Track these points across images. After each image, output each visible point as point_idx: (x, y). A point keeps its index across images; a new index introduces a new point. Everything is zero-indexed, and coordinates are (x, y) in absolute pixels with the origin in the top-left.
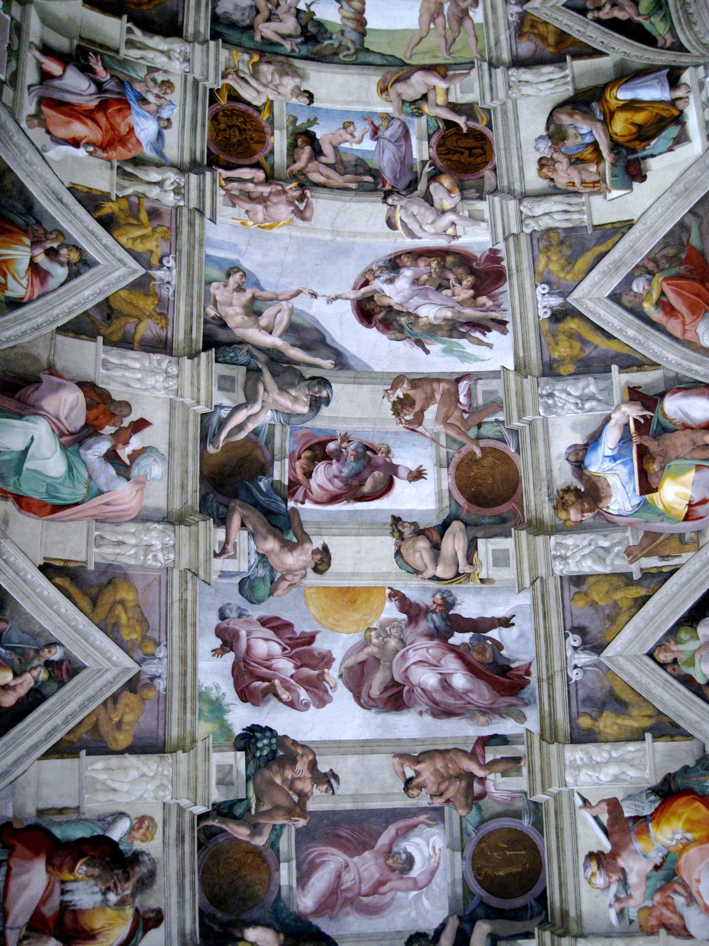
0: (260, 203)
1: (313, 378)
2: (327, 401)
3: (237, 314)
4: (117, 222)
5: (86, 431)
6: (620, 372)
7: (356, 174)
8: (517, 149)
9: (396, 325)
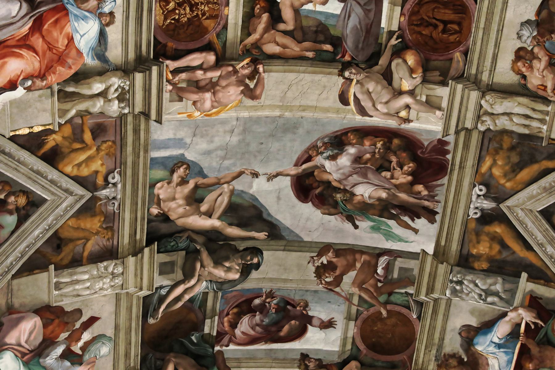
0: (208, 91)
1: (246, 249)
2: (257, 266)
3: (180, 206)
4: (62, 153)
5: (44, 345)
6: (528, 281)
7: (315, 42)
8: (498, 31)
9: (331, 201)
